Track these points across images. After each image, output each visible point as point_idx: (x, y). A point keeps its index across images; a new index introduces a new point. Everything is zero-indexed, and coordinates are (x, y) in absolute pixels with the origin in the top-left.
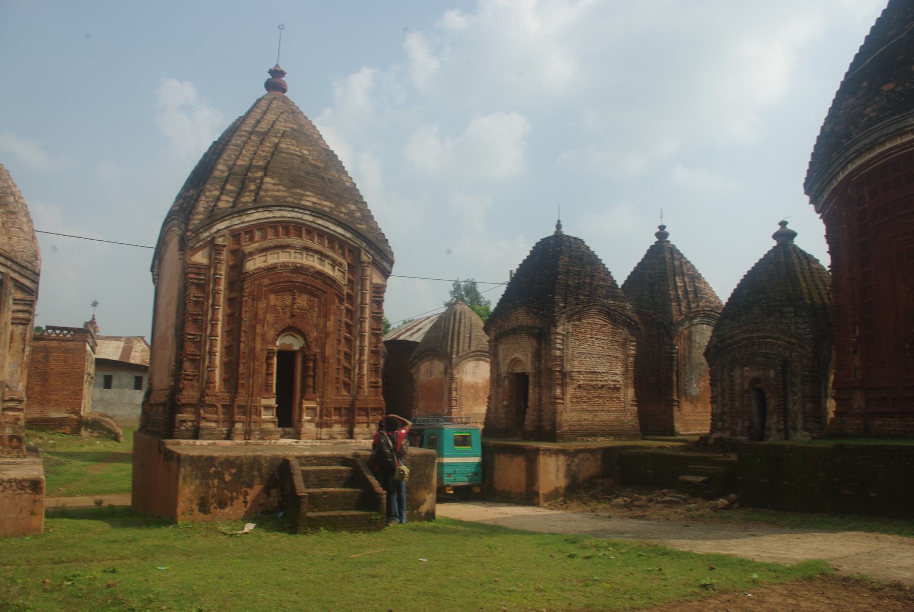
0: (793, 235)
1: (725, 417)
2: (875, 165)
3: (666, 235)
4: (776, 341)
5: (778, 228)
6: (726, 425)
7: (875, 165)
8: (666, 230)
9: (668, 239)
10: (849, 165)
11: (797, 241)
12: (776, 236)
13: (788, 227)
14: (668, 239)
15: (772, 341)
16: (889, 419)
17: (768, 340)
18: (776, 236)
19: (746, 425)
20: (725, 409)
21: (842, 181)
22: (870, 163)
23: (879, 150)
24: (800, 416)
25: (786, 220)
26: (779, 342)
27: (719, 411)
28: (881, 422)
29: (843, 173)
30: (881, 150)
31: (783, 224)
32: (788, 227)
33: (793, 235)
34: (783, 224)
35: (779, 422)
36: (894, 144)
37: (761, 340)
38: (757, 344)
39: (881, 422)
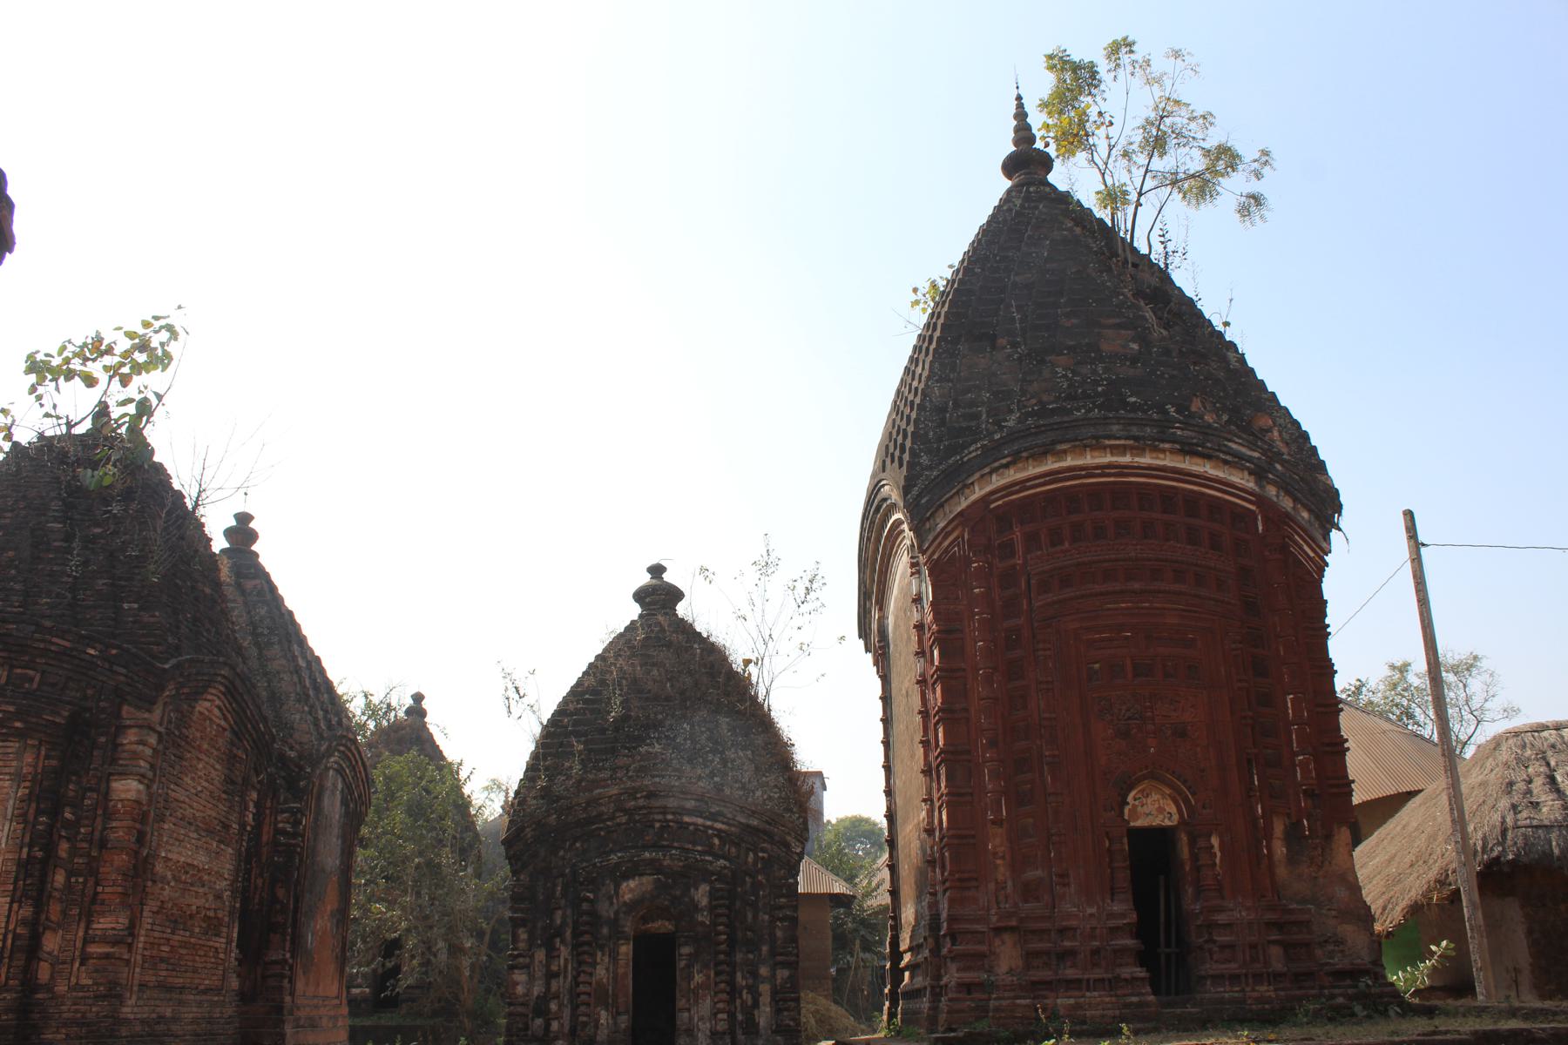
0: (675, 595)
1: (553, 1006)
2: (1038, 490)
3: (253, 536)
4: (709, 823)
5: (645, 579)
6: (555, 1025)
7: (1038, 490)
8: (252, 525)
9: (254, 548)
10: (994, 477)
11: (682, 609)
12: (640, 596)
13: (667, 577)
14: (254, 548)
15: (700, 821)
16: (1088, 994)
17: (686, 819)
18: (640, 596)
19: (623, 1026)
20: (554, 985)
21: (975, 503)
22: (1028, 484)
23: (1051, 465)
24: (765, 999)
25: (664, 563)
26: (719, 826)
27: (537, 989)
28: (1072, 1001)
29: (980, 489)
30: (1057, 466)
31: (657, 570)
32: (667, 577)
33: (675, 595)
34: (657, 570)
35: (715, 1014)
36: (1079, 462)
37: (670, 817)
38: (657, 825)
39: (1072, 1001)
